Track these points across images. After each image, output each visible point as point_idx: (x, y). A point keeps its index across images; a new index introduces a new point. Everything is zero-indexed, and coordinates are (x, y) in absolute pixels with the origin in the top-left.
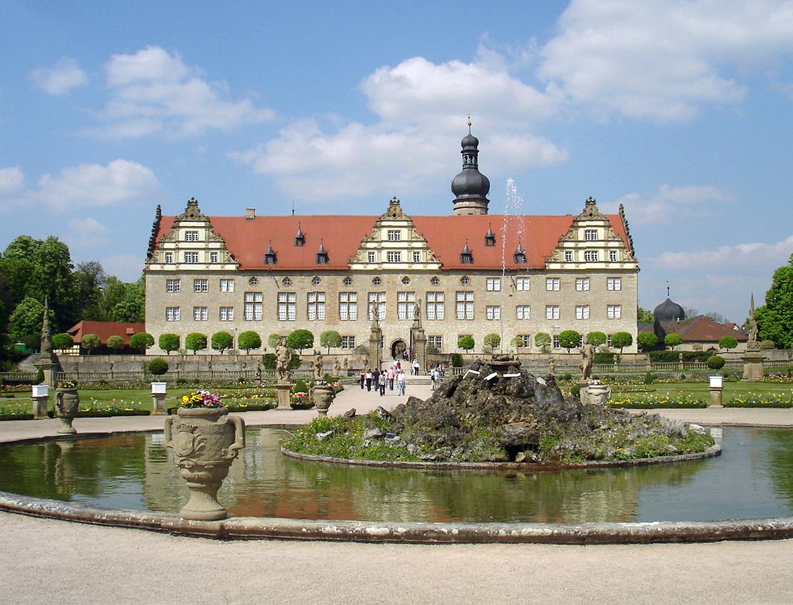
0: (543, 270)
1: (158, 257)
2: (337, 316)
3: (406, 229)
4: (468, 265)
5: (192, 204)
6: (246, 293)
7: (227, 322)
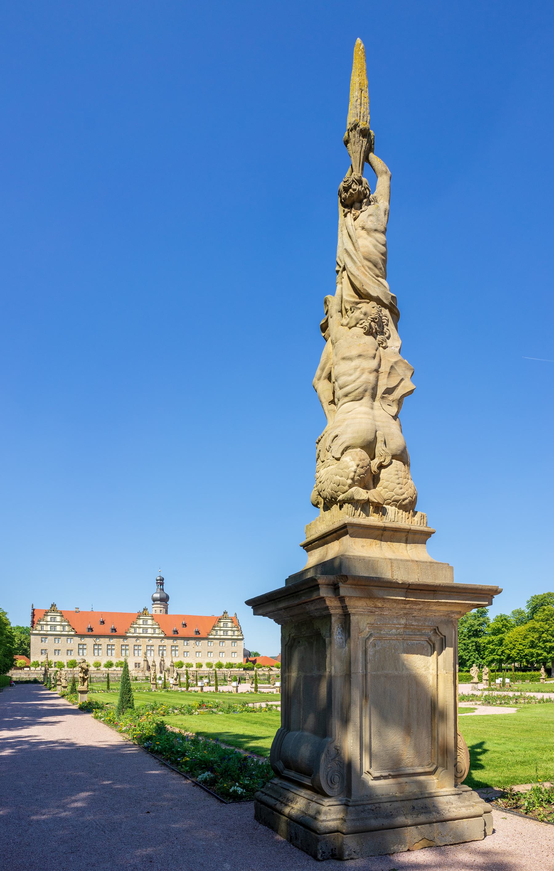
3: (150, 620)
4: (176, 635)
6: (79, 644)
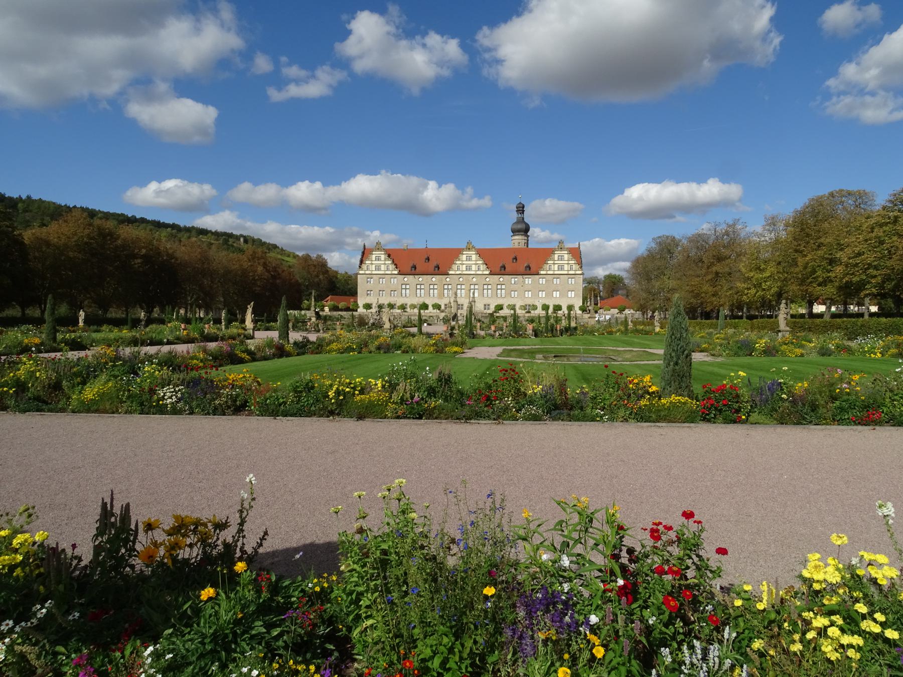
0: (538, 274)
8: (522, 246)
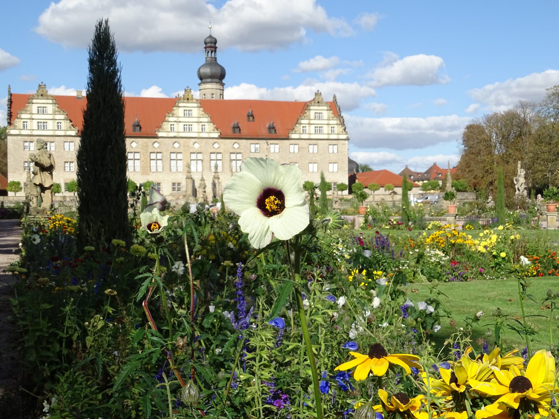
0: (288, 139)
1: (17, 125)
2: (148, 169)
3: (196, 109)
5: (41, 86)
7: (70, 172)
8: (216, 97)
